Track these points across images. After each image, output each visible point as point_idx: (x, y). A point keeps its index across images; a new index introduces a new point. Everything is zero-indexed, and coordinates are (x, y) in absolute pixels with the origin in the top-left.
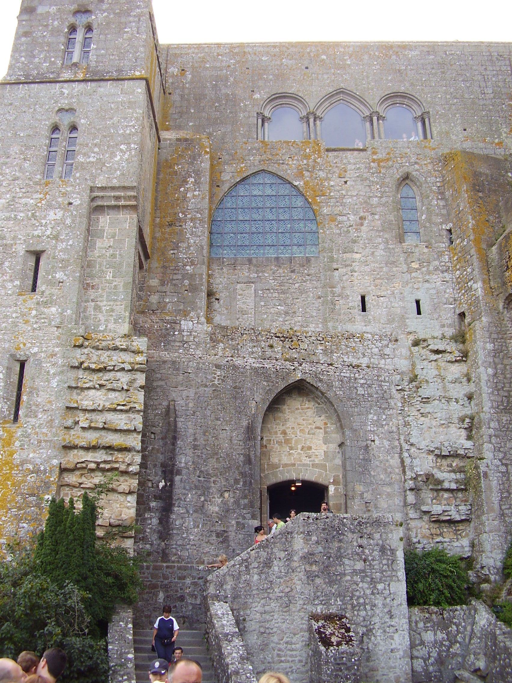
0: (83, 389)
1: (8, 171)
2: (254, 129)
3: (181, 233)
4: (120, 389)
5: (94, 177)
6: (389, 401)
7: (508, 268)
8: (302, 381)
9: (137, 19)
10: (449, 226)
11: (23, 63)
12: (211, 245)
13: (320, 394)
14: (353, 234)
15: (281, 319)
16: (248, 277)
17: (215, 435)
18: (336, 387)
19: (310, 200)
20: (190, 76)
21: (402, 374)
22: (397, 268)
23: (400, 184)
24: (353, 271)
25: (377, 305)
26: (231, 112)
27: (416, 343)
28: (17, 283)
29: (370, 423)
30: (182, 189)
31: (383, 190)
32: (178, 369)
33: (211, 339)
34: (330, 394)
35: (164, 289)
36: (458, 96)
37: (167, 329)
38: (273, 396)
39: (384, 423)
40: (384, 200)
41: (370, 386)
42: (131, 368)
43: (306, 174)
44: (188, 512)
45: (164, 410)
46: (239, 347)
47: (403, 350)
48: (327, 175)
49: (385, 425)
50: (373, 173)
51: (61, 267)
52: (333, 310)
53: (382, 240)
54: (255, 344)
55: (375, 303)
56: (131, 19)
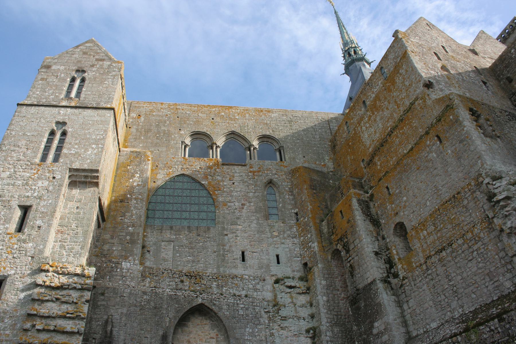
0: (43, 301)
1: (15, 155)
4: (71, 302)
5: (72, 162)
6: (260, 319)
7: (333, 233)
8: (202, 305)
9: (112, 77)
10: (296, 210)
11: (38, 95)
12: (147, 217)
13: (214, 314)
14: (237, 214)
15: (190, 265)
17: (139, 341)
18: (225, 310)
19: (211, 193)
21: (268, 301)
23: (266, 186)
24: (236, 236)
25: (252, 258)
27: (277, 282)
29: (247, 334)
30: (131, 180)
31: (256, 188)
32: (117, 294)
33: (142, 275)
34: (220, 314)
35: (112, 241)
36: (300, 139)
37: (112, 267)
38: (181, 314)
39: (257, 334)
40: (256, 194)
41: (247, 309)
42: (81, 287)
43: (210, 177)
45: (104, 322)
46: (161, 281)
47: (268, 286)
49: (257, 335)
50: (250, 179)
51: (41, 217)
52: (223, 260)
54: (172, 280)
55: (251, 256)
56: (109, 77)
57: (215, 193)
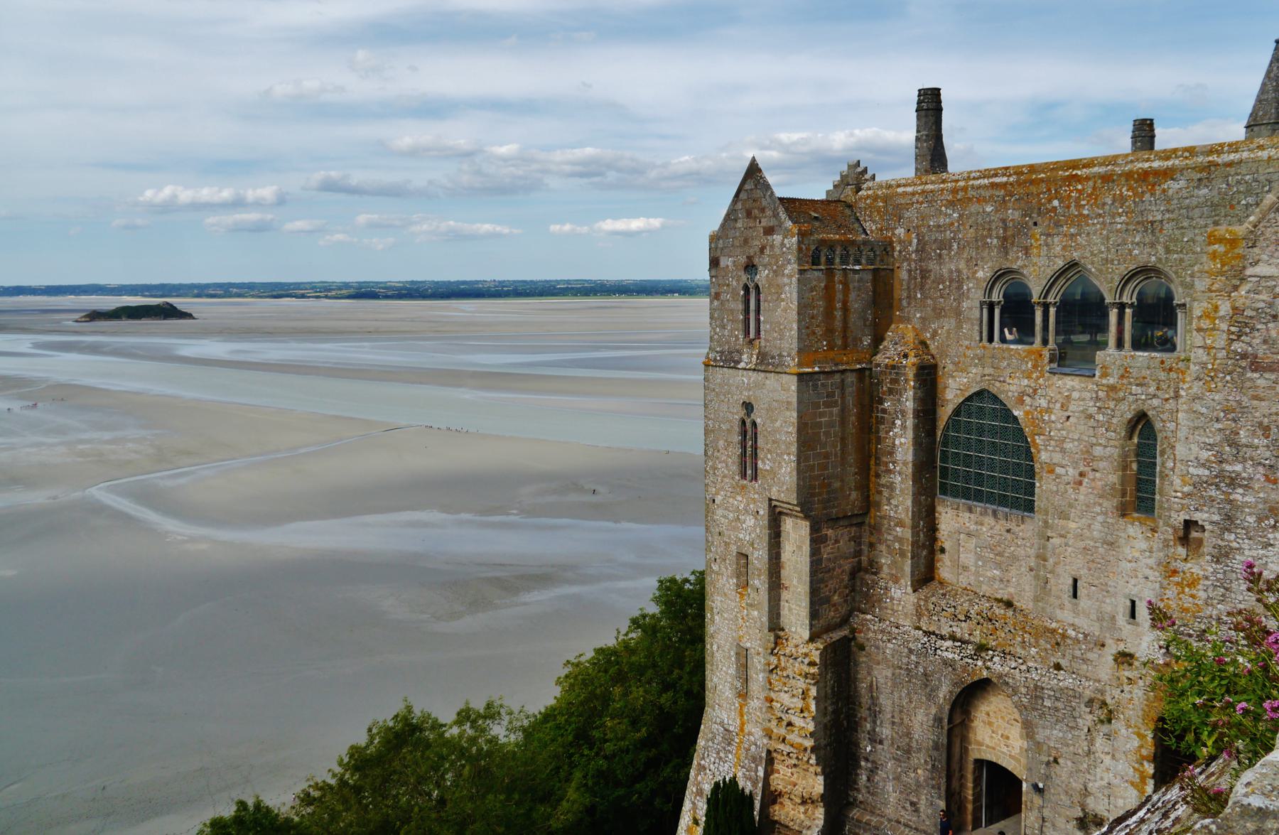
2: (977, 328)
3: (891, 487)
6: (1078, 720)
16: (968, 528)
22: (1114, 553)
26: (955, 300)
30: (891, 433)
41: (1057, 699)
44: (888, 778)
50: (1099, 408)
57: (1034, 441)
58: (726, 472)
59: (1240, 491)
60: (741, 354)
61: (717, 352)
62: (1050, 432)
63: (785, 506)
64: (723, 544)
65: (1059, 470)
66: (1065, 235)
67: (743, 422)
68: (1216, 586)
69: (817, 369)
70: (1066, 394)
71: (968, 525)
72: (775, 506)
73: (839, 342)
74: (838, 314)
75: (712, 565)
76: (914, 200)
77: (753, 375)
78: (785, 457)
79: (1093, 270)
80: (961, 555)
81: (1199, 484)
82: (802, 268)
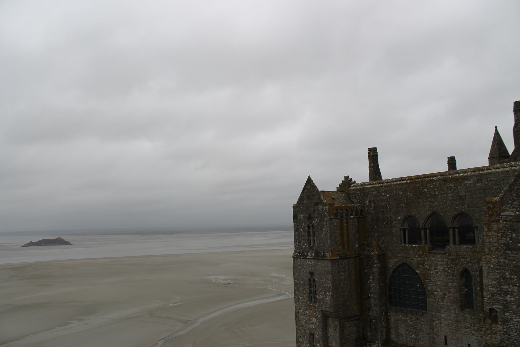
20: (373, 206)
22: (460, 325)
28: (309, 345)
30: (369, 282)
40: (454, 284)
48: (429, 268)
50: (449, 268)
53: (453, 308)
57: (425, 282)
58: (303, 300)
59: (509, 296)
60: (308, 253)
61: (298, 252)
62: (431, 279)
63: (328, 313)
64: (303, 330)
65: (435, 293)
66: (430, 202)
67: (310, 280)
68: (504, 334)
69: (338, 257)
70: (436, 263)
71: (401, 317)
72: (324, 313)
73: (346, 246)
74: (345, 235)
75: (299, 339)
76: (372, 190)
77: (313, 261)
78: (328, 293)
79: (442, 215)
80: (399, 330)
81: (493, 294)
82: (330, 218)
